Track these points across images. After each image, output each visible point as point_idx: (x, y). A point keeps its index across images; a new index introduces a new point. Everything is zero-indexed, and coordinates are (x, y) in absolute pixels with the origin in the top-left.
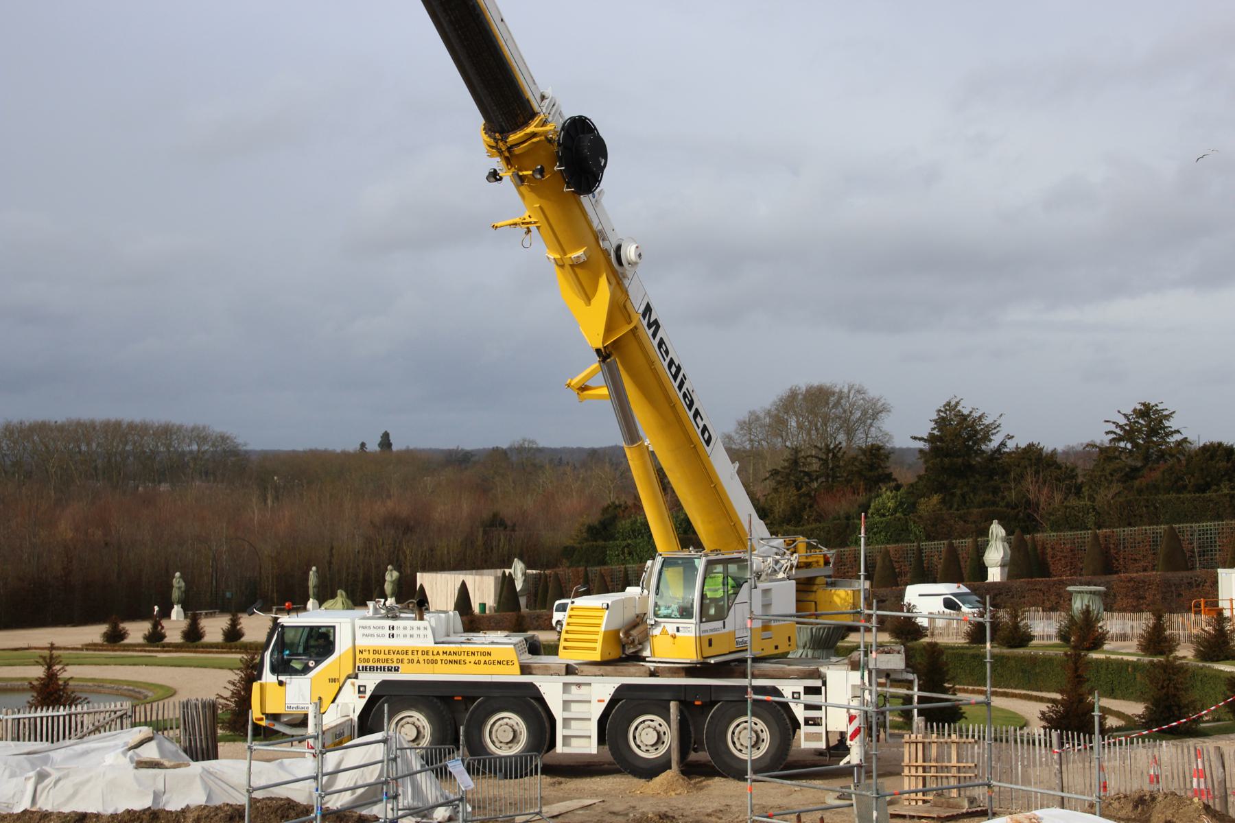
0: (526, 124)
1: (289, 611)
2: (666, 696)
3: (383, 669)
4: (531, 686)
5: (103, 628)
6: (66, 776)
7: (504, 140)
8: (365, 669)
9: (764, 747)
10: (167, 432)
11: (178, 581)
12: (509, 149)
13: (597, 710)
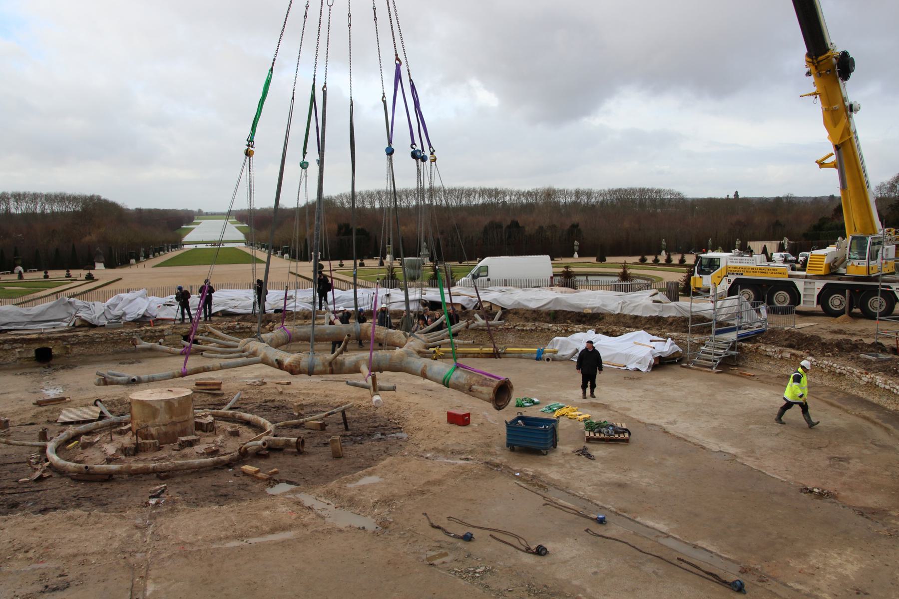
0: (826, 53)
1: (704, 253)
5: (639, 257)
7: (816, 59)
10: (659, 192)
11: (664, 243)
12: (818, 62)
13: (817, 292)
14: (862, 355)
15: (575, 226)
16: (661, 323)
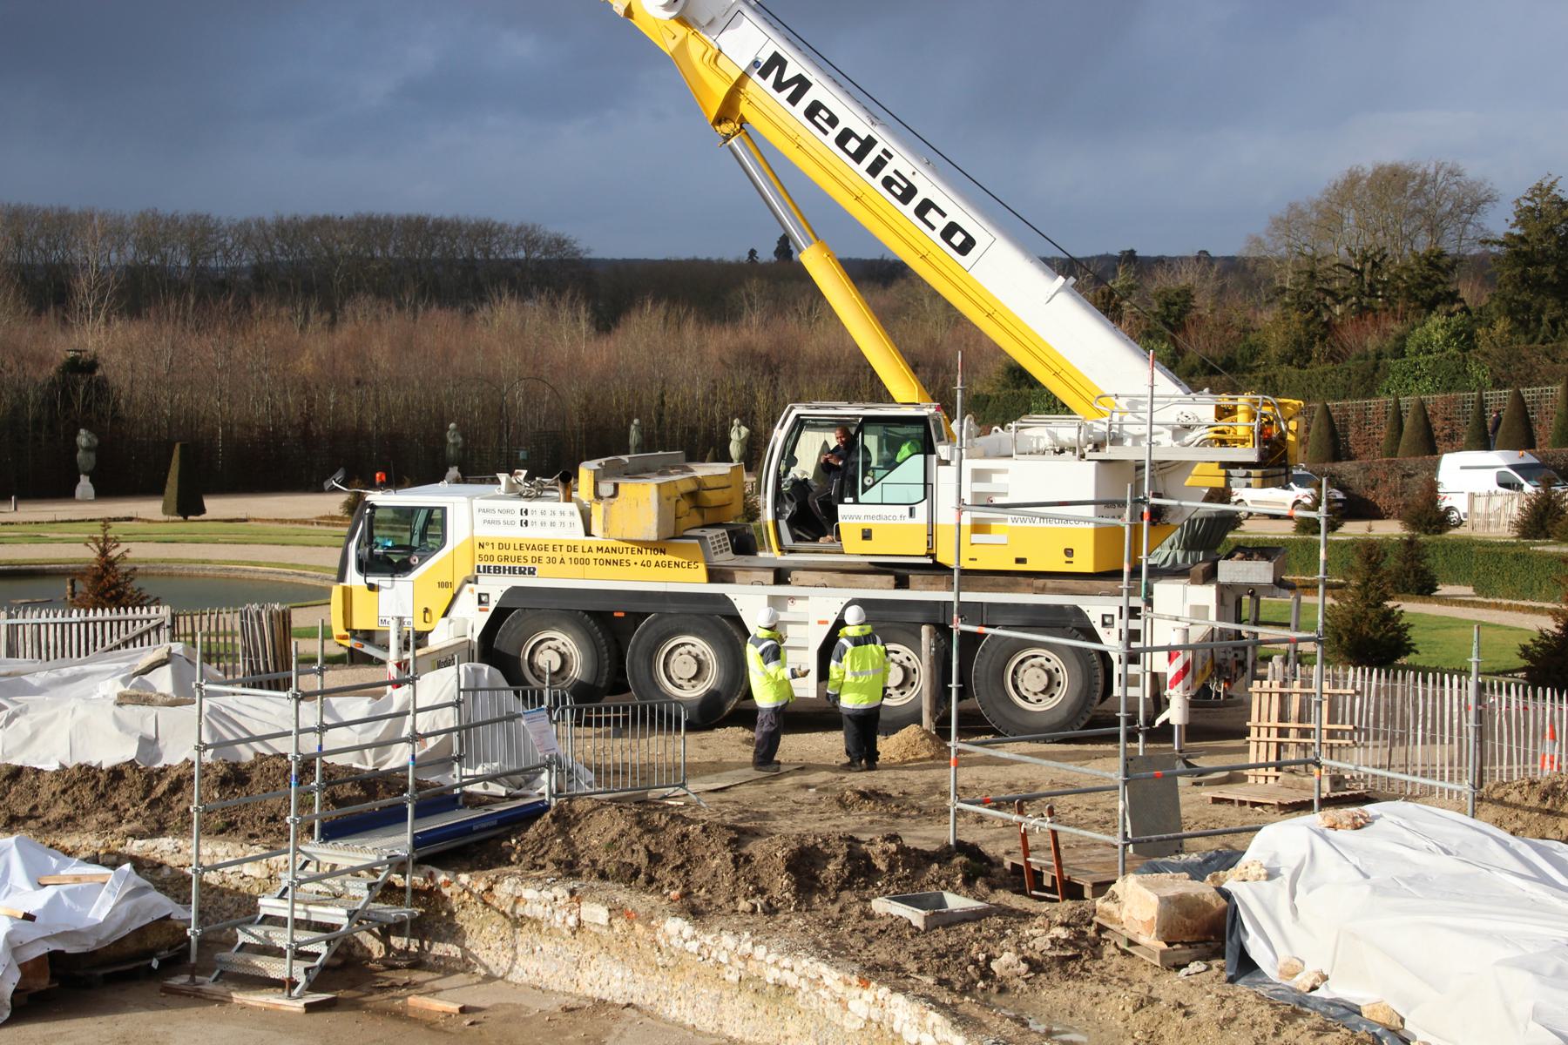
2: (918, 616)
3: (512, 570)
4: (723, 599)
6: (24, 711)
8: (487, 570)
9: (1060, 694)
10: (484, 232)
14: (880, 905)
15: (81, 367)
16: (120, 797)
